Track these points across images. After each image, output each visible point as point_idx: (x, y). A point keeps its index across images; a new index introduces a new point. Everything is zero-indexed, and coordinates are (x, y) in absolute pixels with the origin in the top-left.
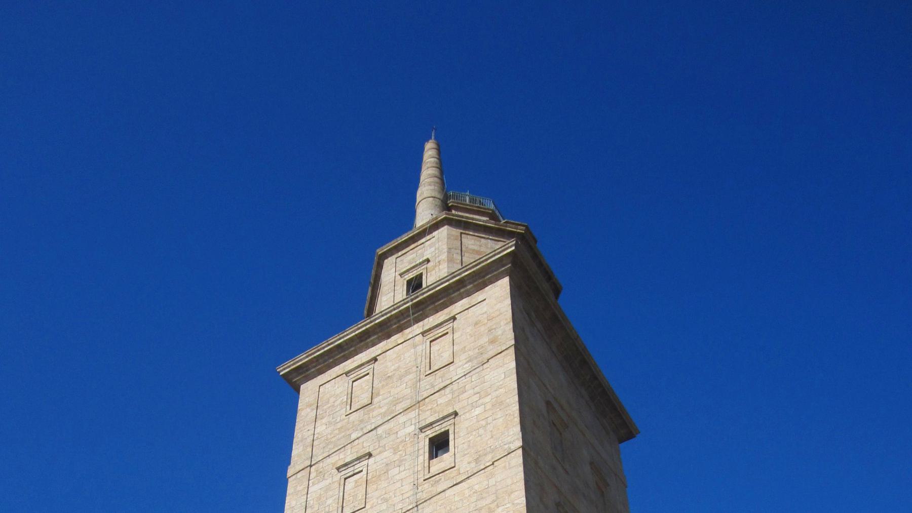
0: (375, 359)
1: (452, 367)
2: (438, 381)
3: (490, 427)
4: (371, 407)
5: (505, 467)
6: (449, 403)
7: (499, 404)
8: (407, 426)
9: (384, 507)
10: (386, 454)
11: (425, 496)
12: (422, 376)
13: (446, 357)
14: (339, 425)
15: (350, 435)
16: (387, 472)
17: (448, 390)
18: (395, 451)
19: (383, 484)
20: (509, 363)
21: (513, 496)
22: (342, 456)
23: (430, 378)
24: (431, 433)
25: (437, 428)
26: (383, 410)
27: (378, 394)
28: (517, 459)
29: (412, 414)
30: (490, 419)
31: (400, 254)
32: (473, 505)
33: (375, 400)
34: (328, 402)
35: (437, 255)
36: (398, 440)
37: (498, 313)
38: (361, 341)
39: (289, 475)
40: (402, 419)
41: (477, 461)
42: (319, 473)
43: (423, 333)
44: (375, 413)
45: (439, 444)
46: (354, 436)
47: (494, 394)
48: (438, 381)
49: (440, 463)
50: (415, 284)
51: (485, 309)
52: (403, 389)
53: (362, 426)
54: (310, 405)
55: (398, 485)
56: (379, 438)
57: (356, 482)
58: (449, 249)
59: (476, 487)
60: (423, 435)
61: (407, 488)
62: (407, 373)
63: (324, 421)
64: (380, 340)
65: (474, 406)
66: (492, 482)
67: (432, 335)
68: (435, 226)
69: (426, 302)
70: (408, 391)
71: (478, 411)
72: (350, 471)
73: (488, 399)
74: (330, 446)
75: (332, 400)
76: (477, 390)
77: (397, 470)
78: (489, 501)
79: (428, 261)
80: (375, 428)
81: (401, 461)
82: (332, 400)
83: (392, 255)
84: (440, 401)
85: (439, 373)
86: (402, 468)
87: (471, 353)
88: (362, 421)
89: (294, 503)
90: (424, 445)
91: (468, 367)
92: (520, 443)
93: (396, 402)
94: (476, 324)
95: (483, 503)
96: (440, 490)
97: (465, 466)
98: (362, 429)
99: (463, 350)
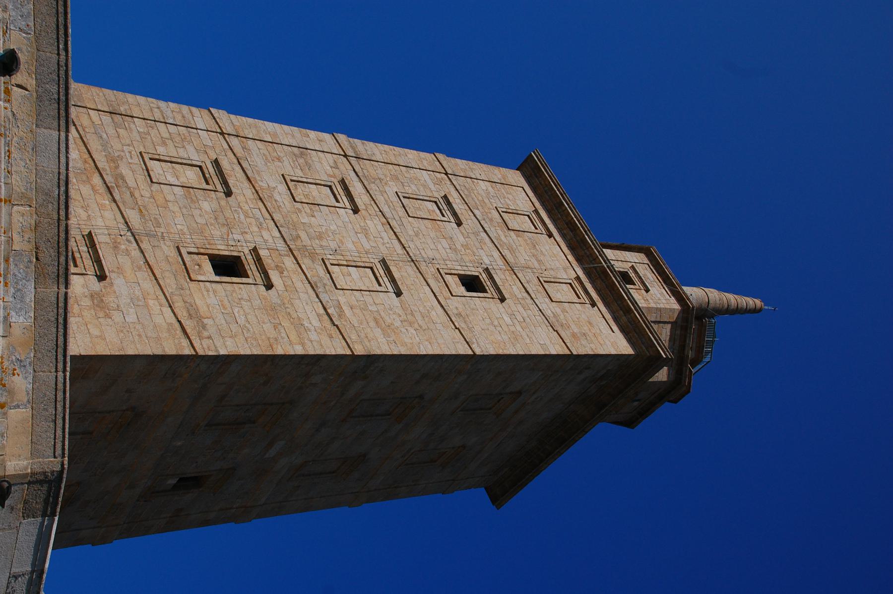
0: (550, 235)
1: (547, 300)
2: (533, 287)
3: (492, 328)
4: (505, 230)
5: (454, 338)
6: (513, 295)
7: (515, 337)
8: (489, 257)
9: (411, 233)
10: (461, 238)
11: (423, 267)
12: (537, 275)
13: (556, 296)
14: (486, 201)
16: (444, 238)
17: (526, 295)
18: (466, 246)
19: (433, 234)
20: (556, 349)
22: (458, 201)
23: (536, 280)
24: (484, 277)
25: (488, 283)
26: (503, 238)
27: (518, 236)
28: (463, 349)
29: (500, 262)
30: (500, 329)
32: (416, 309)
33: (512, 233)
34: (507, 193)
35: (654, 298)
36: (475, 251)
37: (602, 342)
38: (567, 224)
40: (496, 254)
41: (459, 315)
42: (441, 180)
43: (578, 278)
44: (500, 232)
45: (472, 284)
46: (476, 212)
47: (524, 334)
48: (533, 287)
50: (626, 278)
51: (604, 332)
52: (523, 256)
54: (504, 177)
55: (433, 246)
56: (476, 234)
57: (434, 211)
58: (660, 310)
59: (433, 313)
60: (481, 271)
61: (431, 254)
62: (539, 261)
63: (490, 189)
65: (512, 315)
66: (439, 326)
67: (576, 284)
68: (681, 298)
69: (610, 290)
70: (523, 262)
71: (507, 319)
73: (519, 328)
74: (466, 192)
75: (510, 197)
76: (528, 320)
78: (421, 323)
79: (647, 290)
80: (485, 231)
81: (455, 250)
82: (510, 197)
85: (541, 289)
86: (448, 251)
87: (562, 317)
88: (491, 220)
89: (410, 156)
90: (472, 271)
91: (548, 313)
92: (478, 352)
93: (511, 249)
94: (590, 323)
95: (419, 318)
96: (430, 281)
97: (453, 305)
99: (564, 311)
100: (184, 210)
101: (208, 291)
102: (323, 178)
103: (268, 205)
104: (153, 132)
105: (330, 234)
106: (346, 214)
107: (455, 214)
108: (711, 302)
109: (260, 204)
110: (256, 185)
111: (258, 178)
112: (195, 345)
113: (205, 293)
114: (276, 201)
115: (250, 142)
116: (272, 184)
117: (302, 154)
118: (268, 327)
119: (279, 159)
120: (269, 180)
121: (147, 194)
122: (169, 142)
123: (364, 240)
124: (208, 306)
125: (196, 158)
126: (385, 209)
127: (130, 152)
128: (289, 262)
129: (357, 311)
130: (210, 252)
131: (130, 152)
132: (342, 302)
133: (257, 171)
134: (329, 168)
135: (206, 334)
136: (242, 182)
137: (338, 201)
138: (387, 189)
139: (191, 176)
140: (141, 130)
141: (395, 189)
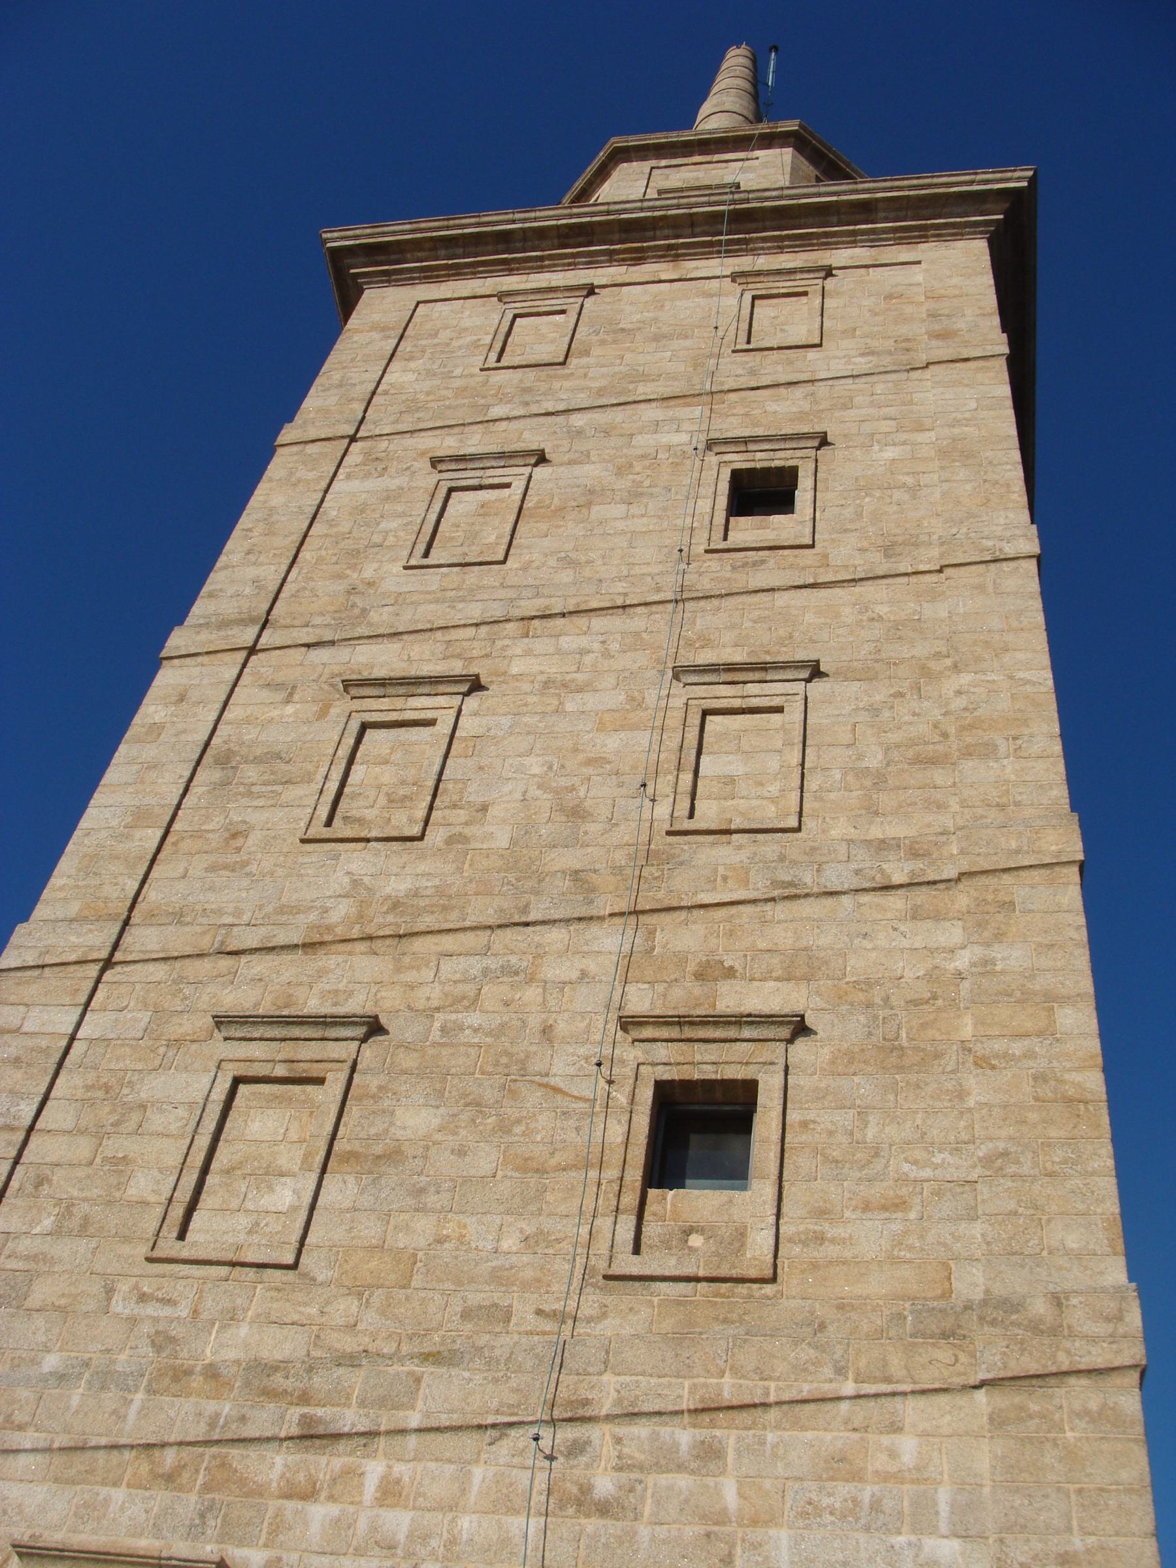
0: (591, 290)
4: (560, 371)
11: (705, 585)
14: (458, 383)
15: (488, 407)
17: (799, 392)
21: (1007, 659)
26: (595, 385)
31: (663, 163)
33: (573, 362)
39: (281, 440)
42: (371, 458)
46: (497, 411)
49: (747, 530)
53: (527, 398)
59: (883, 610)
64: (612, 258)
71: (890, 453)
72: (470, 477)
77: (619, 510)
83: (644, 159)
84: (772, 407)
86: (634, 509)
89: (277, 500)
96: (754, 584)
98: (527, 404)
100: (431, 1199)
101: (820, 1238)
102: (330, 734)
103: (427, 921)
104: (64, 1185)
105: (563, 782)
106: (477, 715)
107: (507, 457)
108: (745, 113)
109: (419, 944)
110: (340, 931)
111: (313, 917)
112: (1100, 1362)
113: (832, 1251)
114: (416, 893)
115: (152, 894)
116: (339, 881)
117: (224, 761)
118: (979, 1089)
119: (236, 834)
120: (332, 884)
121: (345, 1307)
122: (115, 1146)
123: (590, 701)
124: (895, 1261)
125: (193, 1084)
126: (475, 611)
127: (143, 1298)
128: (684, 938)
129: (885, 800)
130: (635, 1174)
131: (143, 1298)
132: (853, 833)
133: (281, 910)
134: (290, 709)
135: (1040, 1307)
136: (322, 973)
137: (431, 723)
138: (388, 585)
139: (262, 1123)
140: (48, 1223)
141: (397, 568)
